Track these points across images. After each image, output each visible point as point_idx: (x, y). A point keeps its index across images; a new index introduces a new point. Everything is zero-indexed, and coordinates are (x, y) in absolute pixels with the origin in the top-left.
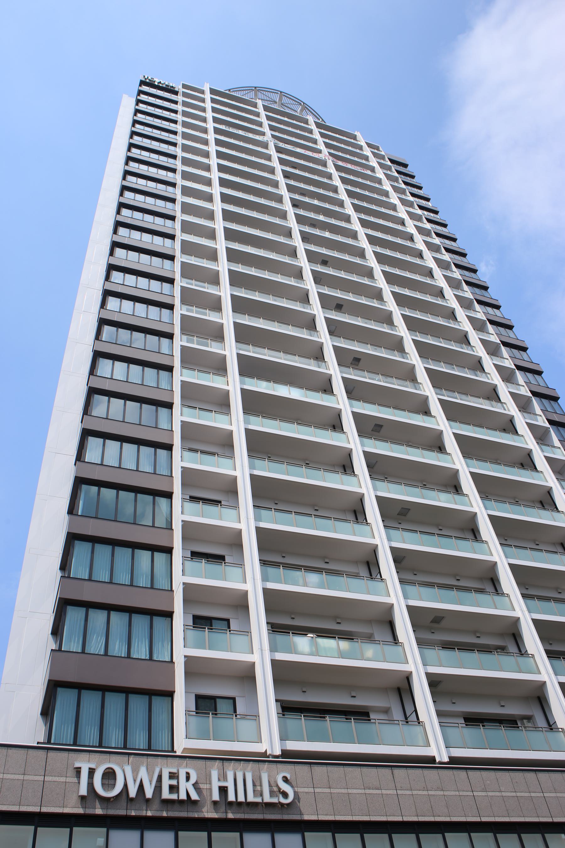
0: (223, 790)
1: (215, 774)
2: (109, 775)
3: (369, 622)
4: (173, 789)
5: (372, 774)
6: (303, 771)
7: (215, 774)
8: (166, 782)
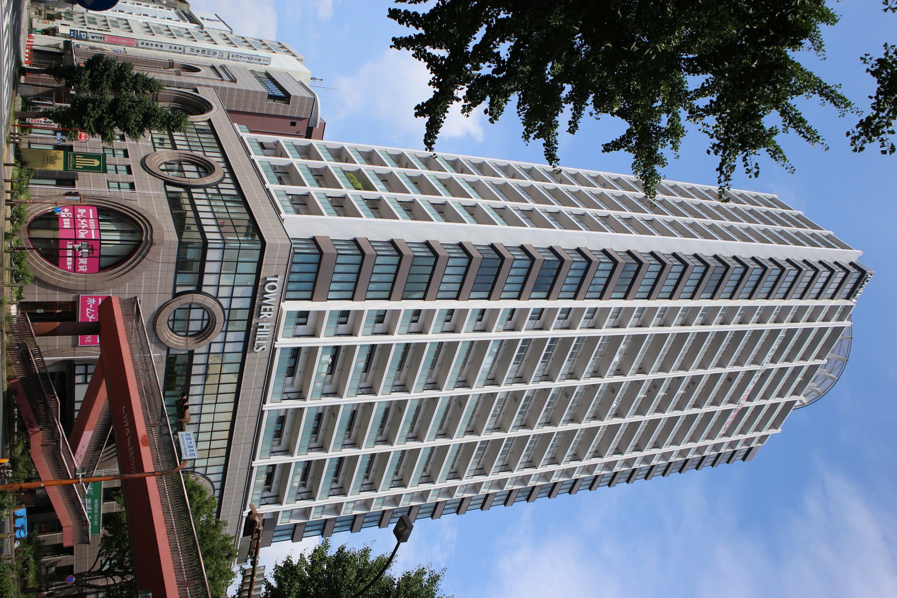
0: (262, 327)
1: (269, 324)
2: (274, 288)
3: (338, 384)
4: (265, 310)
5: (261, 380)
6: (266, 354)
7: (269, 324)
8: (268, 307)
